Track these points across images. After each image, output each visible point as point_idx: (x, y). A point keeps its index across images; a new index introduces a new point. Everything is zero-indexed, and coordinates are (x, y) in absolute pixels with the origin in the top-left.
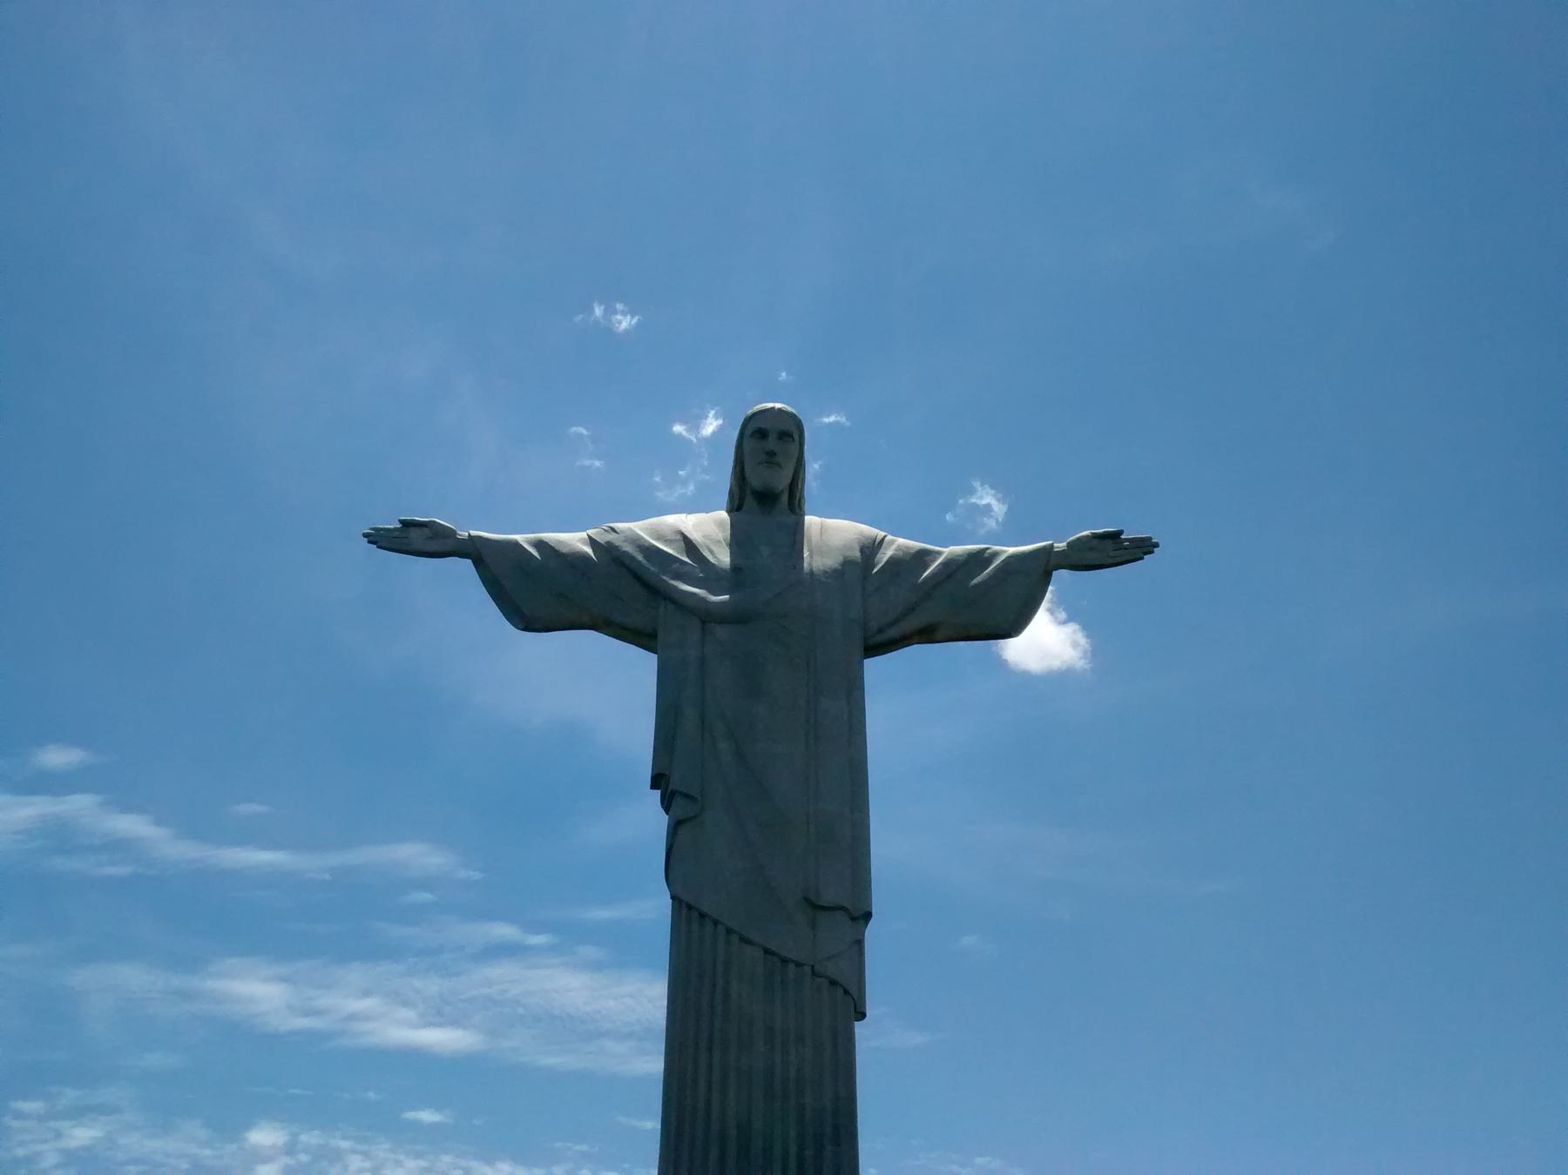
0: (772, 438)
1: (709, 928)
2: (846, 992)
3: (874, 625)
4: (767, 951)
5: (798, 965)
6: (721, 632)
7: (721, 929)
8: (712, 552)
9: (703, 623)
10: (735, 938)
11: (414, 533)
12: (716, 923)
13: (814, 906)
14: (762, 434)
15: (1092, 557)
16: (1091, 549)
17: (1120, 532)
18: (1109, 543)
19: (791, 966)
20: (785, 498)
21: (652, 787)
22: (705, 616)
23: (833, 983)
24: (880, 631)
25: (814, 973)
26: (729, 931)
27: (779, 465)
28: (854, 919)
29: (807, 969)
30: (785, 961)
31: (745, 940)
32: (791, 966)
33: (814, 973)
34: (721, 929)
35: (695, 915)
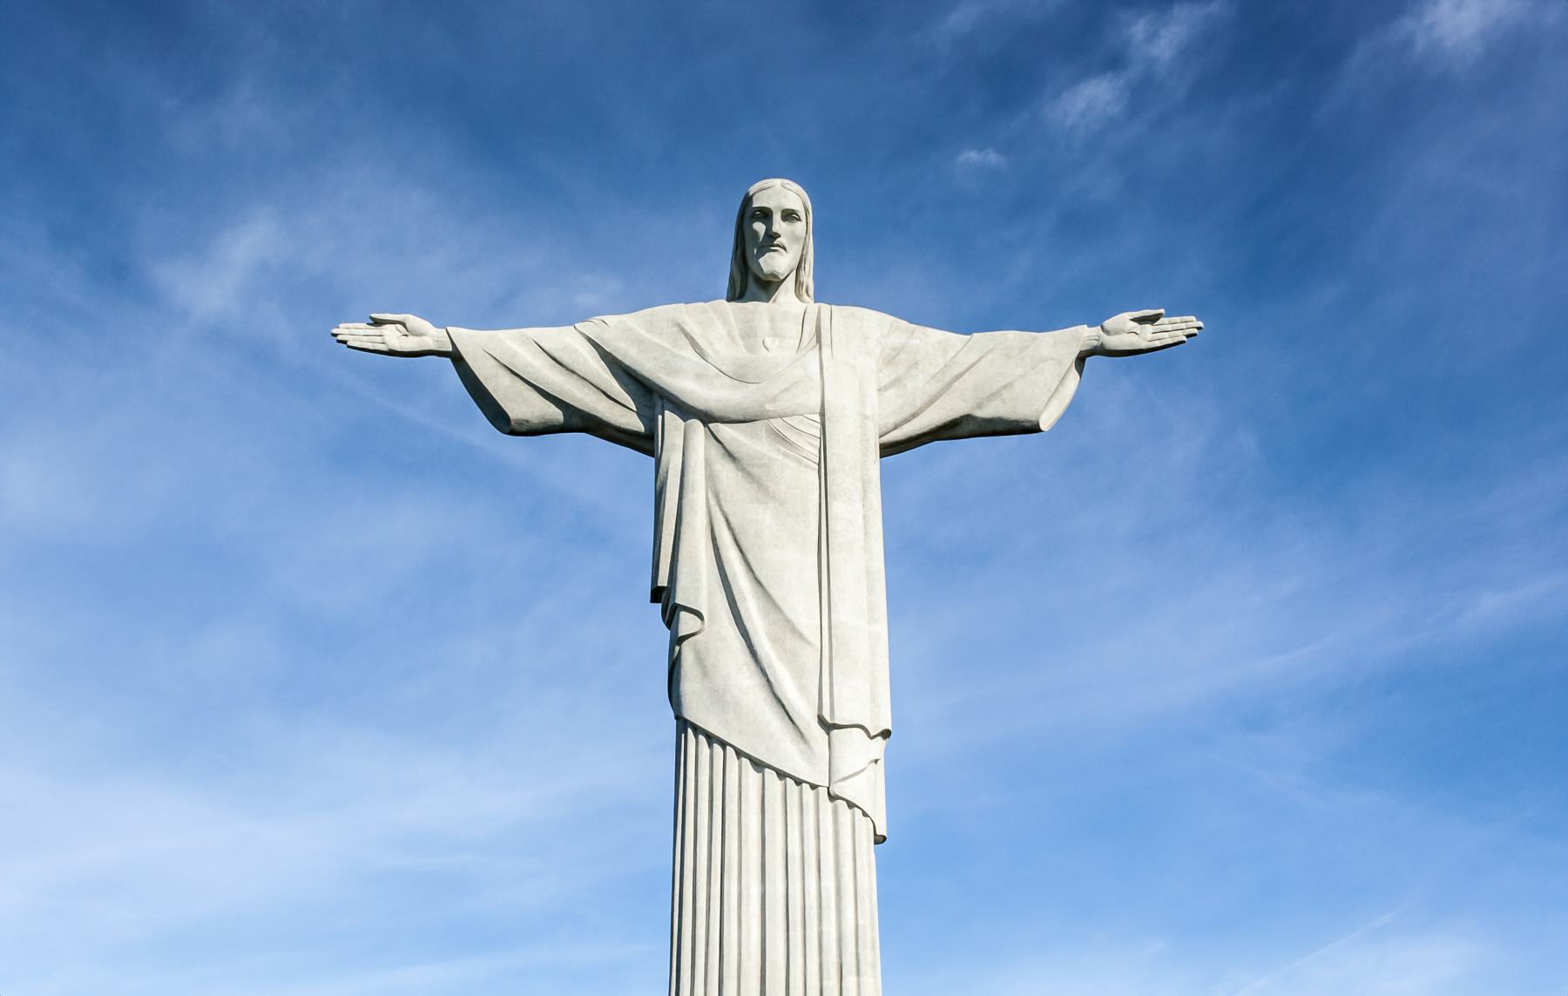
0: (777, 217)
1: (717, 747)
2: (865, 814)
3: (892, 421)
4: (782, 775)
5: (814, 787)
6: (723, 430)
8: (711, 344)
9: (705, 424)
12: (724, 744)
13: (828, 727)
14: (765, 215)
18: (1149, 327)
20: (790, 283)
22: (707, 418)
23: (851, 805)
26: (740, 754)
28: (872, 738)
29: (823, 792)
30: (799, 782)
35: (702, 738)
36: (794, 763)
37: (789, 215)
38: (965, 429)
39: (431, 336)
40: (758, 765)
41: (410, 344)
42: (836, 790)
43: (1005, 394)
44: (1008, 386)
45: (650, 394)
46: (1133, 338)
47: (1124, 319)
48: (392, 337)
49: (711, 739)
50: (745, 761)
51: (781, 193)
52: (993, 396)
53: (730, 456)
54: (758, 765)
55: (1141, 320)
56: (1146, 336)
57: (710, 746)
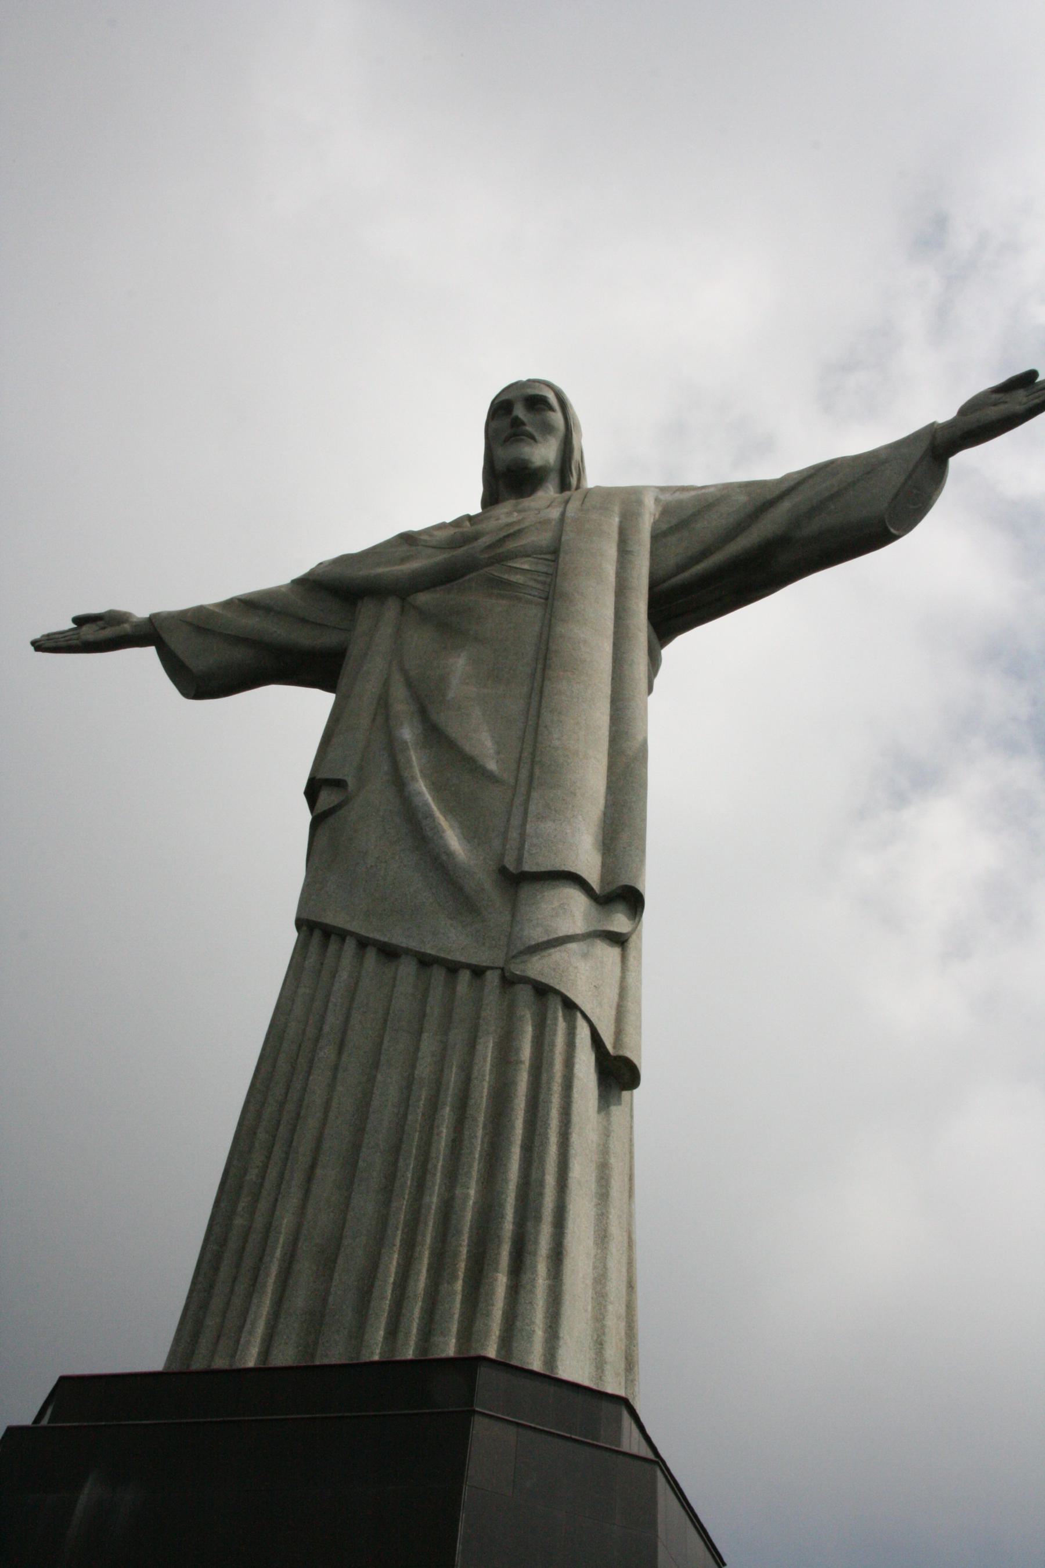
4: (425, 962)
5: (478, 972)
6: (423, 598)
9: (403, 599)
10: (371, 955)
11: (85, 629)
12: (343, 935)
15: (993, 413)
16: (995, 404)
17: (1032, 375)
19: (465, 976)
24: (682, 568)
25: (509, 981)
26: (363, 943)
27: (533, 438)
30: (453, 968)
31: (389, 953)
32: (465, 976)
34: (350, 945)
36: (455, 941)
41: (108, 633)
42: (517, 969)
44: (832, 497)
46: (1002, 407)
48: (89, 633)
52: (816, 509)
53: (424, 616)
57: (325, 946)
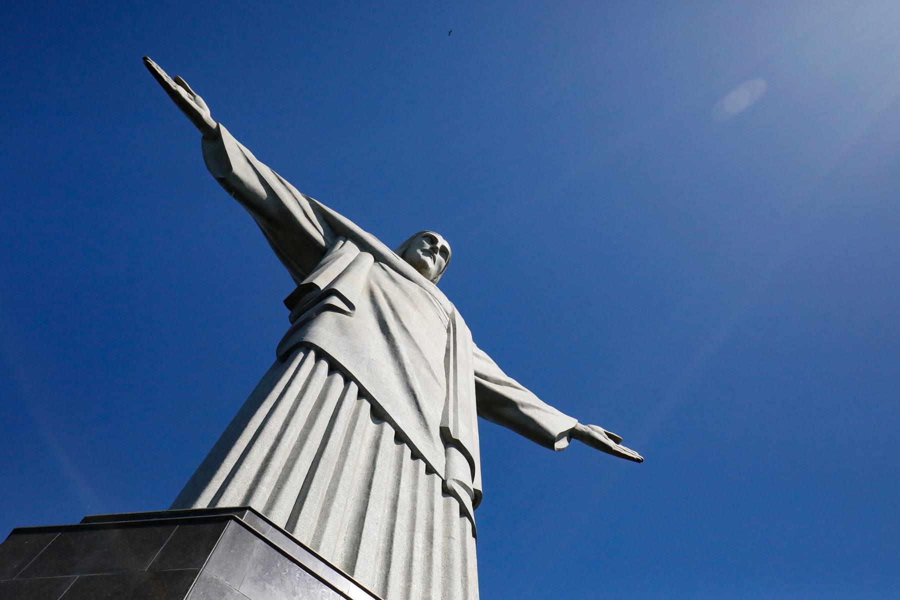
4: (401, 437)
7: (354, 388)
12: (348, 378)
21: (285, 301)
26: (363, 394)
33: (447, 491)
37: (443, 251)
38: (508, 412)
39: (205, 113)
40: (379, 414)
43: (537, 411)
45: (336, 232)
47: (601, 430)
49: (335, 367)
50: (366, 405)
51: (442, 242)
54: (379, 414)
55: (610, 437)
56: (611, 443)
